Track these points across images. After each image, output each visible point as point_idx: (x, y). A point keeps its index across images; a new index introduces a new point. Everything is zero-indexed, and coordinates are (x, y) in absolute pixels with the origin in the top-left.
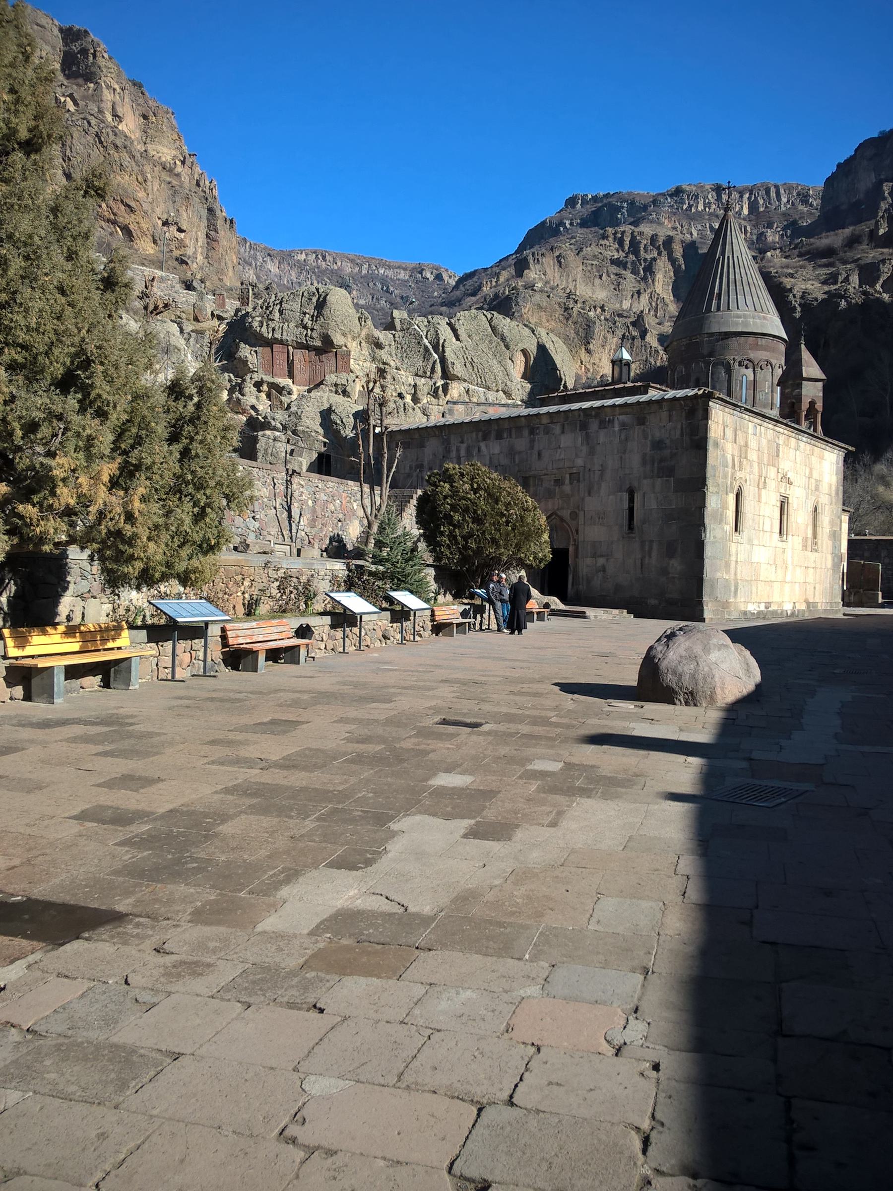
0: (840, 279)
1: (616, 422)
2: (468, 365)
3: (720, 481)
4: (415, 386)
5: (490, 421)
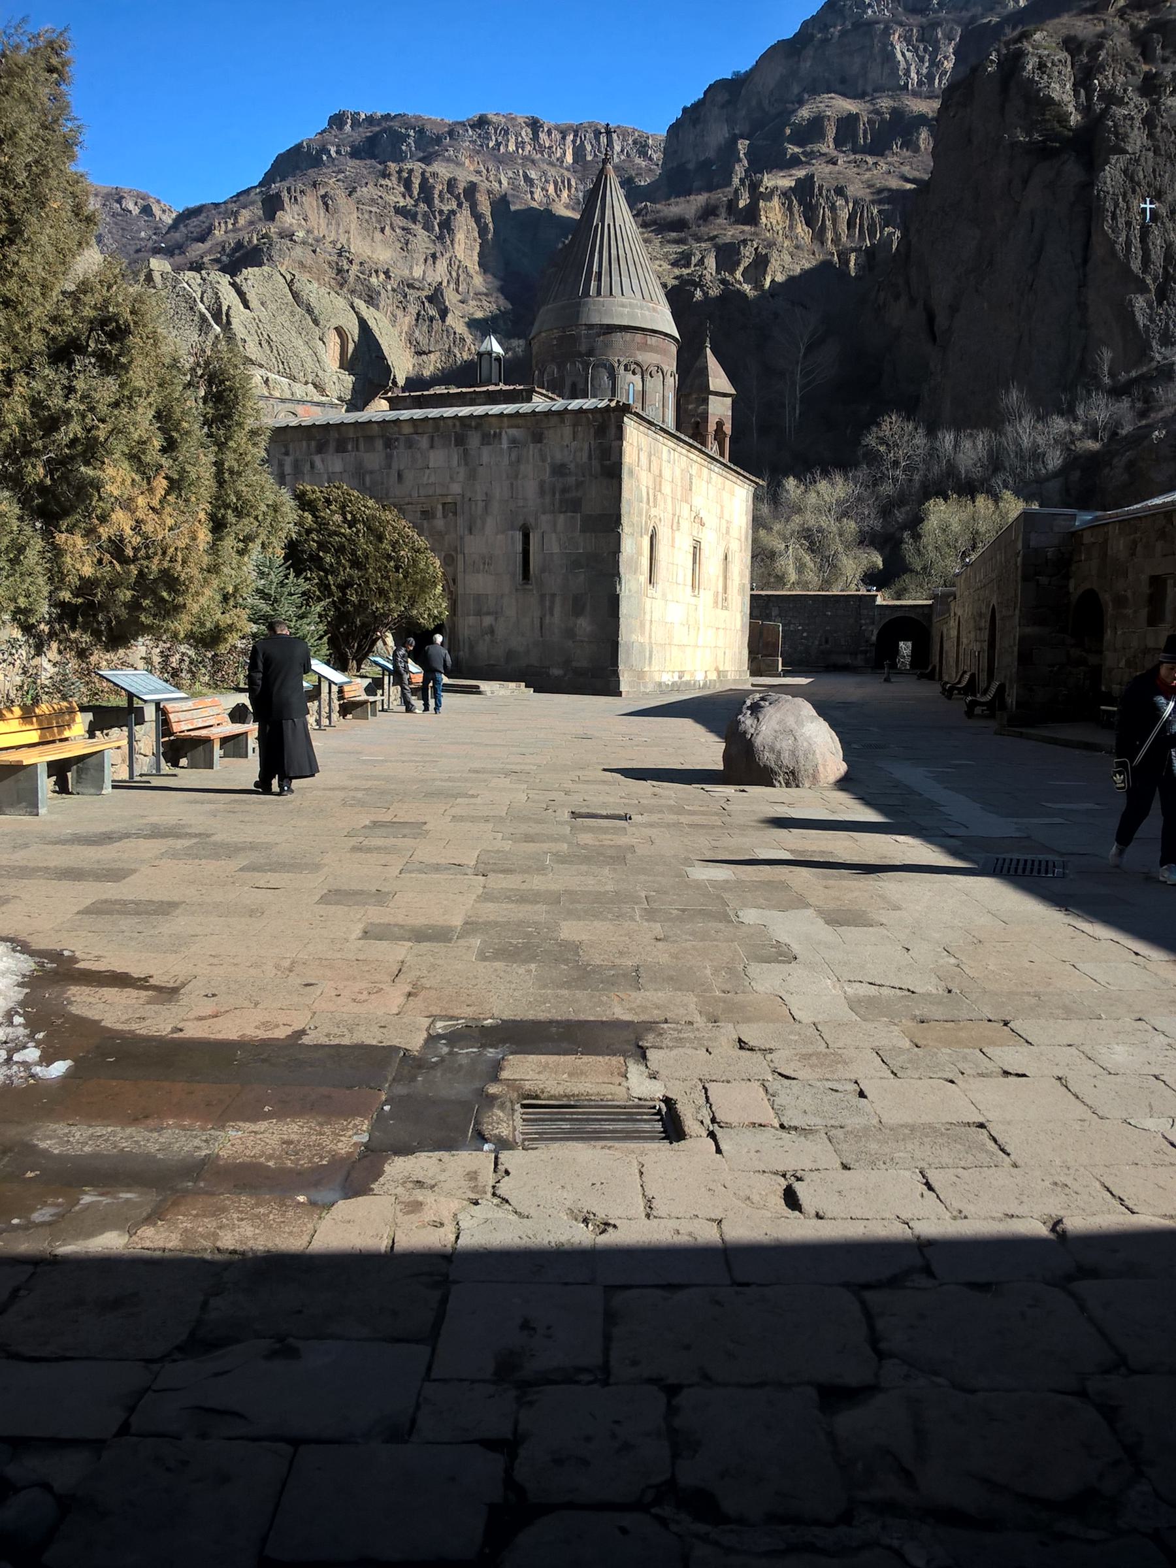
0: (694, 260)
3: (635, 519)
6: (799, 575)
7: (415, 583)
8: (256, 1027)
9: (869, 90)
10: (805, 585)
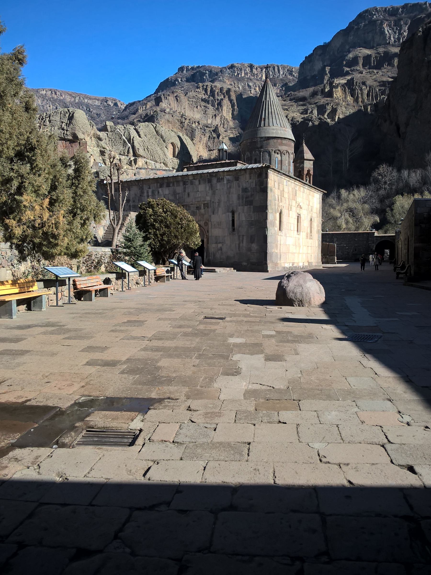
0: (309, 112)
1: (225, 178)
2: (146, 150)
3: (273, 207)
4: (120, 160)
6: (346, 225)
7: (188, 233)
8: (15, 398)
9: (375, 45)
10: (349, 229)
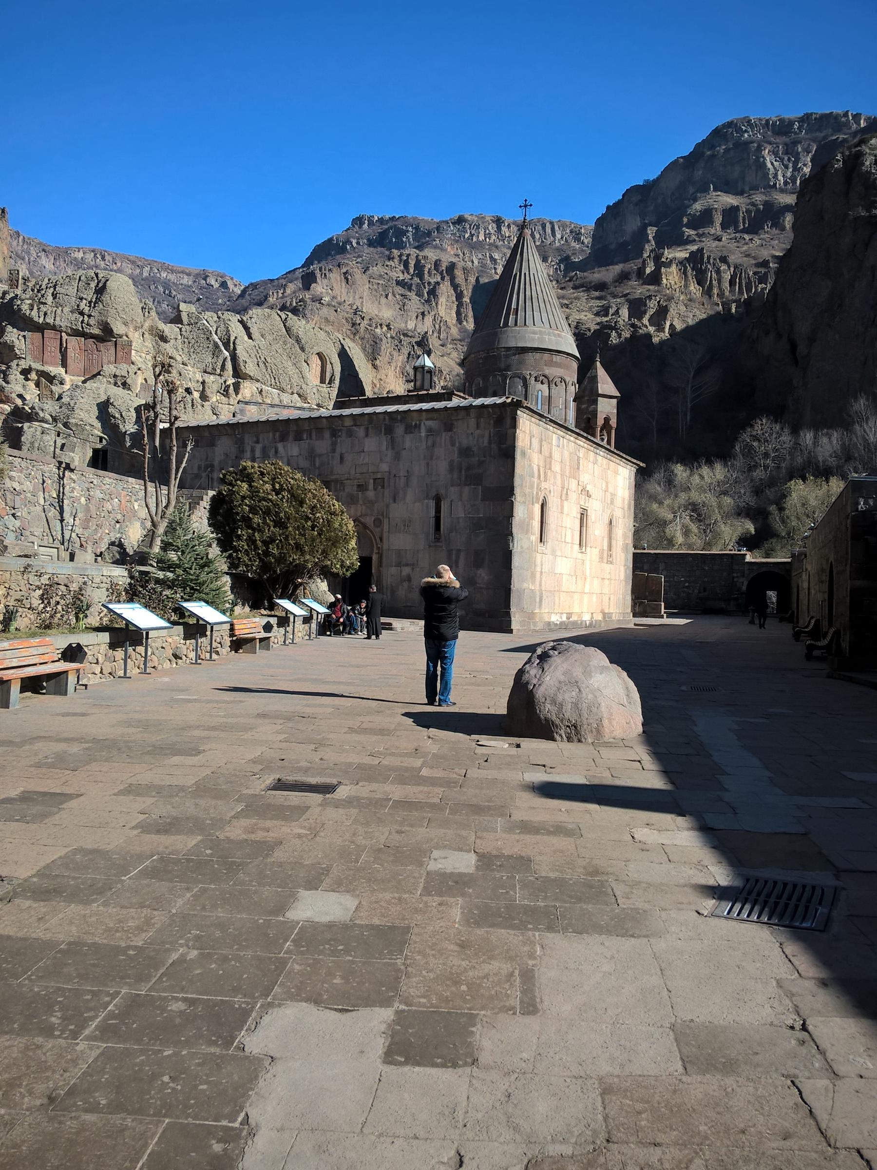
2: (261, 364)
3: (527, 491)
4: (203, 383)
5: (288, 420)
